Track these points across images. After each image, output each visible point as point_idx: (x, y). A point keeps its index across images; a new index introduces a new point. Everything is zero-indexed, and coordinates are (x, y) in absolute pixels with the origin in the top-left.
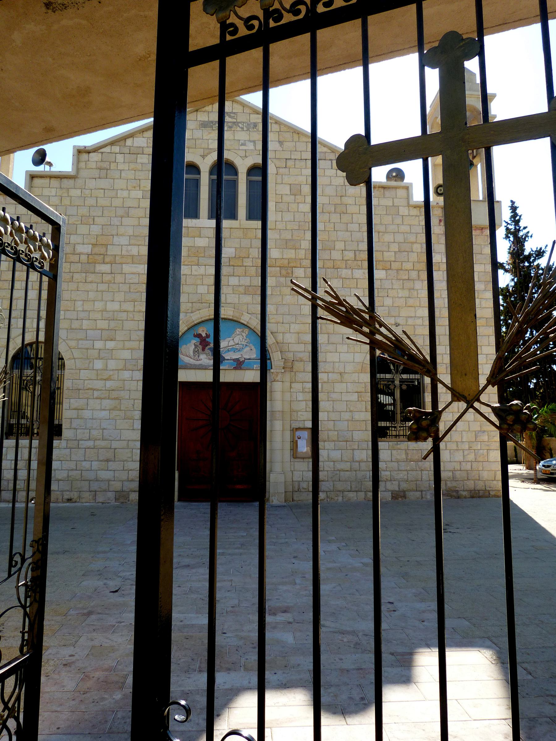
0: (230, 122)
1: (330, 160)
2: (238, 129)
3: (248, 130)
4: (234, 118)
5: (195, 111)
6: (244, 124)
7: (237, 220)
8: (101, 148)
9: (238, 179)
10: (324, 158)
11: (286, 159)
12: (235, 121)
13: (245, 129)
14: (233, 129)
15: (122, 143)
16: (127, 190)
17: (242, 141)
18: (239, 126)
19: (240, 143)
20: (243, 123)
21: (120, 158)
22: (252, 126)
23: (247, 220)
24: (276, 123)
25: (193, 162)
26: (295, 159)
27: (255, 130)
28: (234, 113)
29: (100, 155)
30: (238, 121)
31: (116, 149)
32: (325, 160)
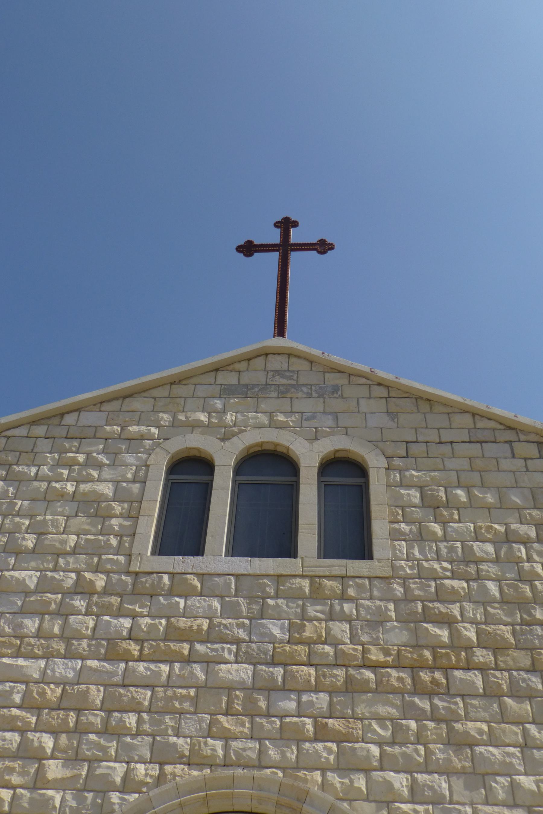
0: (282, 385)
1: (506, 442)
2: (300, 395)
3: (321, 396)
4: (291, 379)
5: (212, 371)
6: (313, 388)
7: (296, 557)
8: (9, 429)
9: (297, 483)
10: (493, 440)
11: (407, 442)
12: (294, 382)
13: (314, 395)
14: (289, 395)
15: (56, 421)
16: (45, 500)
17: (309, 414)
18: (302, 391)
19: (304, 417)
20: (311, 385)
21: (43, 445)
22: (329, 389)
23: (319, 557)
24: (380, 384)
25: (198, 450)
26: (427, 442)
27: (335, 395)
28: (293, 371)
29: (4, 440)
30: (301, 382)
31: (40, 430)
32: (495, 442)
